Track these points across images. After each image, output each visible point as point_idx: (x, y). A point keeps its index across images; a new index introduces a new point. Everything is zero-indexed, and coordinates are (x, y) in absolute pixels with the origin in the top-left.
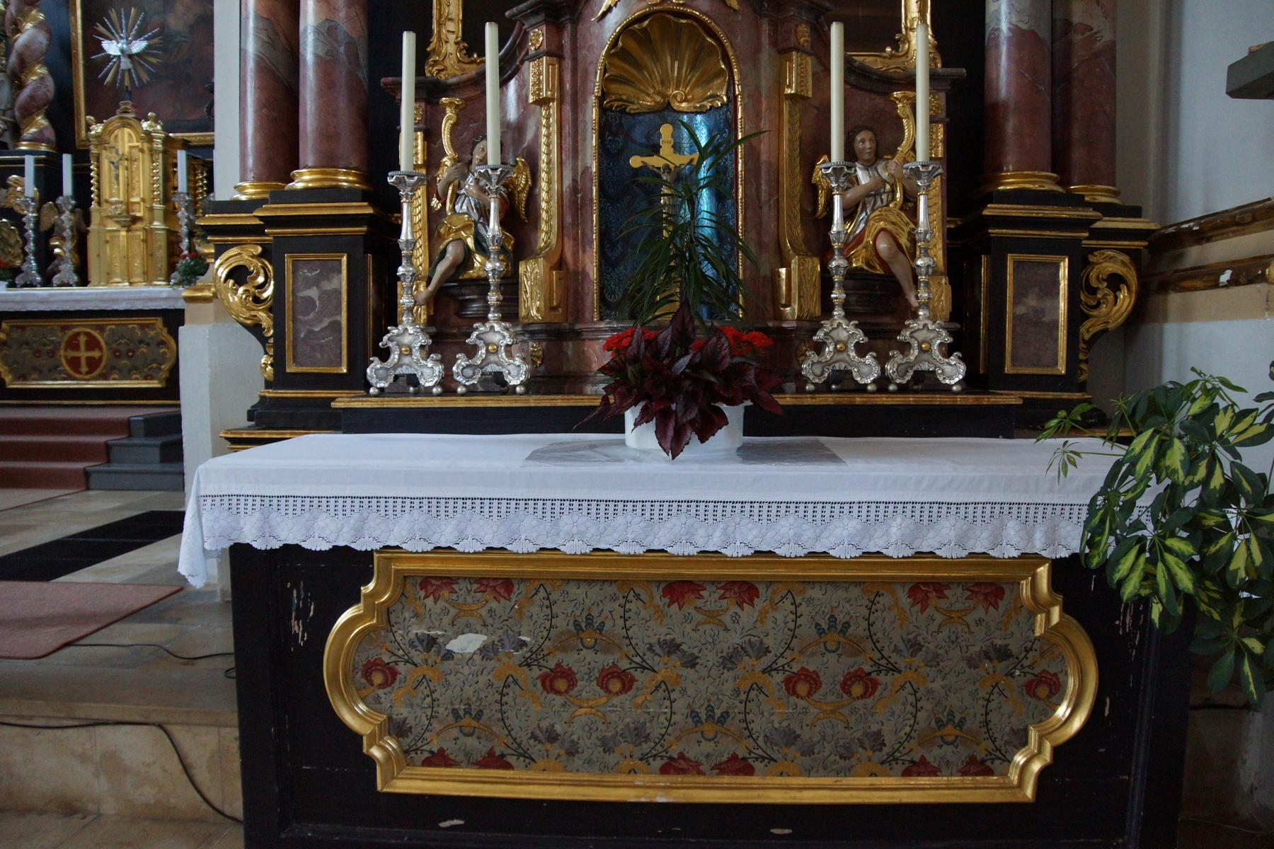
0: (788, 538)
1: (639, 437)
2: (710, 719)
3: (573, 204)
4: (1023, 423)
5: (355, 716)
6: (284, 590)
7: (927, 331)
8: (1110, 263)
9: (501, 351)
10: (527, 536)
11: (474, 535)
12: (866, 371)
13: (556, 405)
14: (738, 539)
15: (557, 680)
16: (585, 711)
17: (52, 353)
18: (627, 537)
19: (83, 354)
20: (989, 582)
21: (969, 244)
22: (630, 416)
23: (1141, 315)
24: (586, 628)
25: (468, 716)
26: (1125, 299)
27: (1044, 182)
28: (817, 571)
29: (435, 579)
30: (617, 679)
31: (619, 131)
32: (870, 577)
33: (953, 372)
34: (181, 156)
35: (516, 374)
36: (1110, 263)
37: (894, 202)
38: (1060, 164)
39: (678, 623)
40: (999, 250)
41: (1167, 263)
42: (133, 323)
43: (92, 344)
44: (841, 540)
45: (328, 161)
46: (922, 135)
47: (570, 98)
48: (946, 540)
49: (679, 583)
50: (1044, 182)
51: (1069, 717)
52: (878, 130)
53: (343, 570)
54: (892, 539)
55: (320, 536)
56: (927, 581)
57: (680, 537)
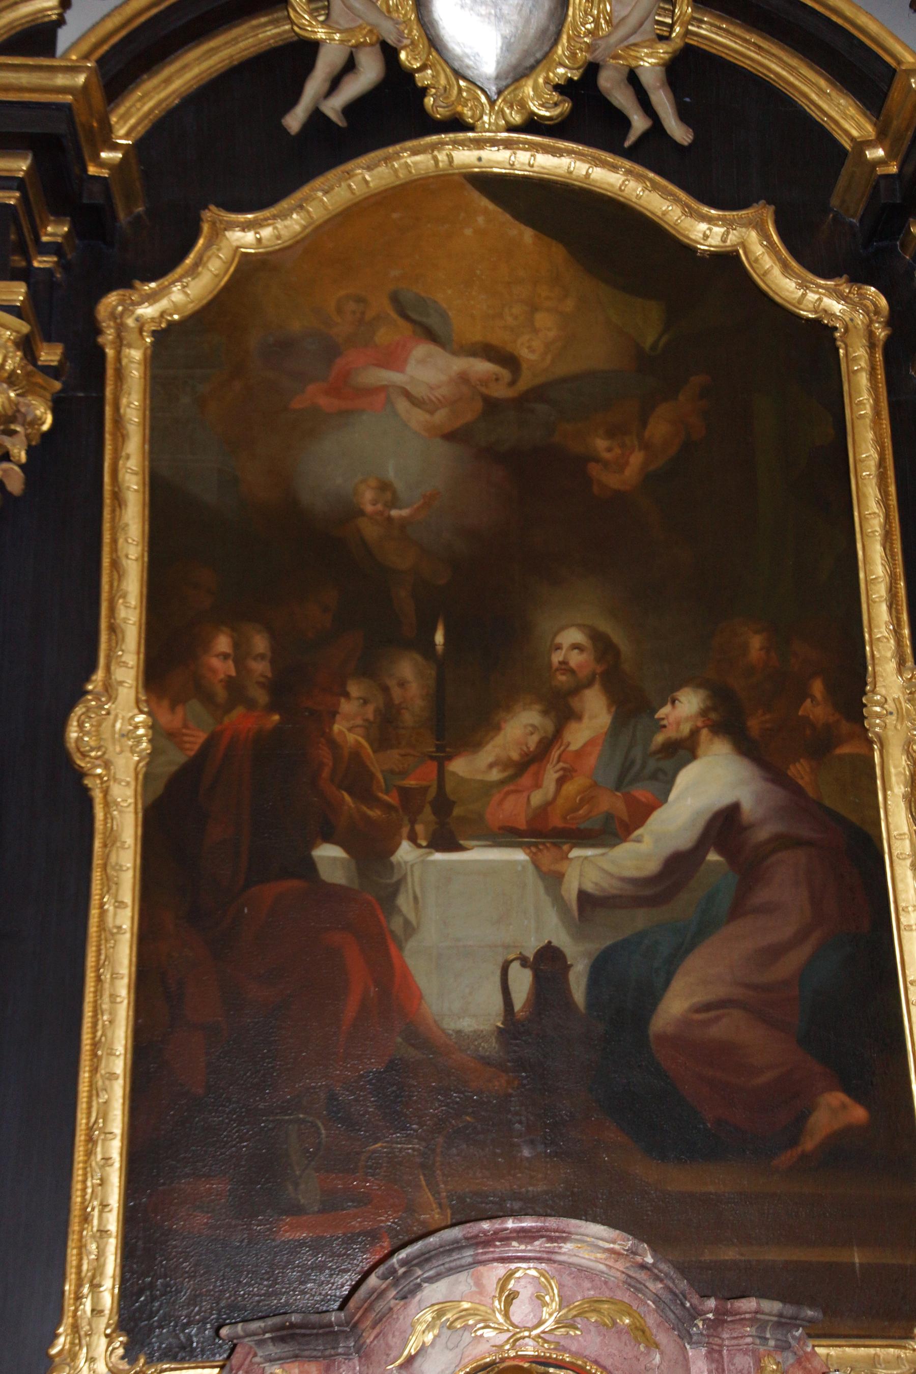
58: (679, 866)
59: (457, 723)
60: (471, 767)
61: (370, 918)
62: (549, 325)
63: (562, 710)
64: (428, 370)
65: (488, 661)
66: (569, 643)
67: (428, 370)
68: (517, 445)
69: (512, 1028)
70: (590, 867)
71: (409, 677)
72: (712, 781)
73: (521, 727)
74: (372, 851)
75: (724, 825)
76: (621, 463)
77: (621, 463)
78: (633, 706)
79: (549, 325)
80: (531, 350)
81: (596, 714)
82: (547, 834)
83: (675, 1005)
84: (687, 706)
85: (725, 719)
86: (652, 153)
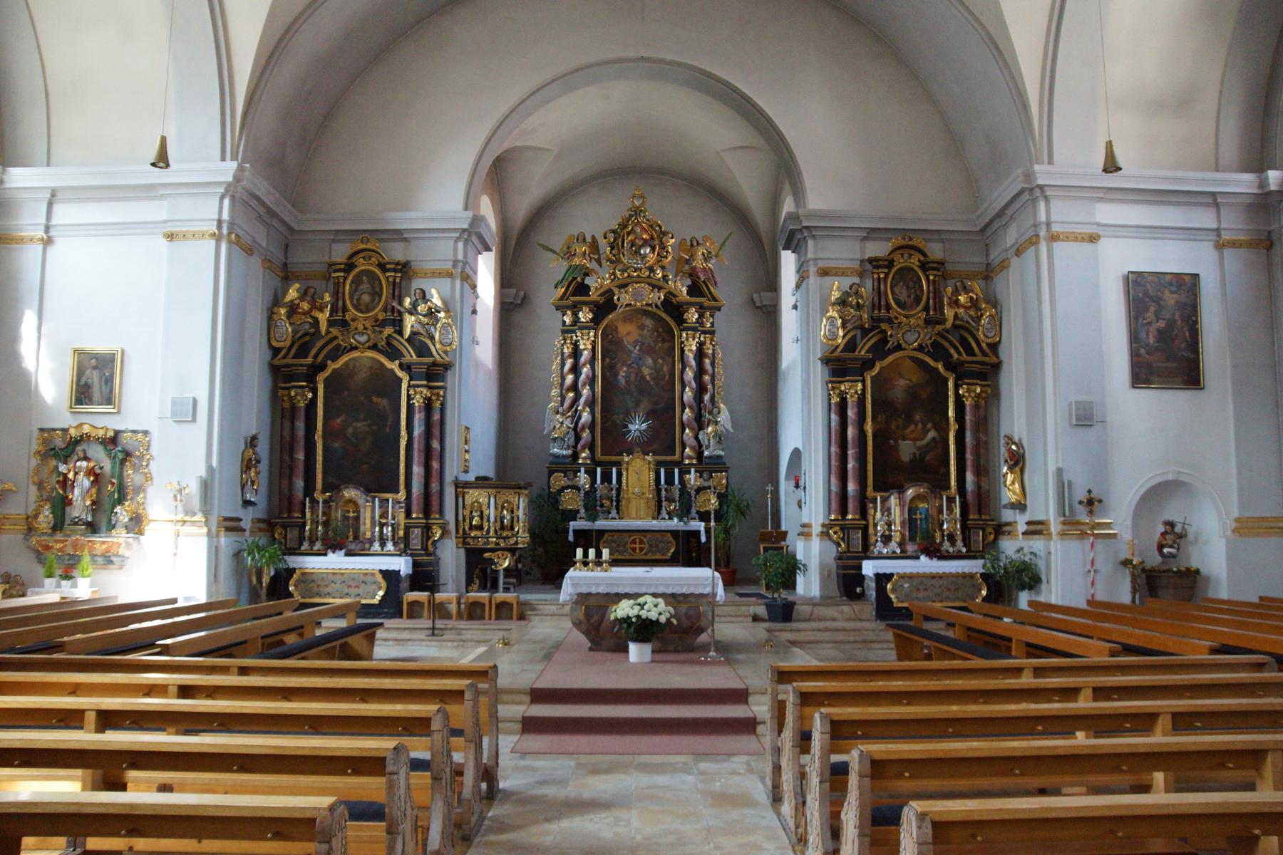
0: (947, 571)
1: (923, 558)
2: (937, 595)
3: (903, 524)
4: (975, 558)
5: (892, 596)
6: (882, 579)
7: (959, 543)
8: (990, 530)
9: (894, 546)
10: (915, 571)
11: (908, 571)
12: (951, 550)
13: (904, 556)
14: (941, 571)
15: (918, 590)
16: (922, 594)
17: (625, 546)
18: (928, 570)
19: (638, 546)
20: (971, 576)
21: (964, 528)
22: (923, 558)
23: (996, 540)
24: (921, 583)
25: (906, 596)
26: (992, 536)
27: (977, 517)
28: (950, 575)
29: (903, 577)
30: (925, 590)
31: (912, 511)
32: (957, 575)
33: (964, 550)
34: (662, 471)
35: (898, 551)
36: (990, 530)
37: (951, 522)
38: (980, 513)
39: (933, 582)
40: (969, 529)
41: (1000, 529)
42: (658, 535)
43: (641, 542)
44: (953, 571)
45: (854, 514)
46: (957, 510)
47: (902, 505)
48: (966, 571)
49: (933, 577)
50: (977, 517)
51: (984, 593)
52: (950, 510)
53: (889, 577)
54: (960, 571)
55: (888, 571)
56: (965, 576)
57: (934, 571)
58: (928, 444)
59: (905, 427)
60: (908, 431)
61: (896, 448)
62: (915, 376)
63: (916, 425)
64: (902, 382)
65: (909, 419)
66: (917, 417)
67: (902, 382)
68: (912, 392)
69: (911, 461)
70: (919, 443)
71: (900, 420)
72: (932, 434)
73: (912, 427)
74: (896, 441)
75: (934, 439)
76: (924, 395)
77: (924, 395)
78: (924, 425)
79: (915, 376)
80: (914, 380)
81: (920, 426)
82: (915, 440)
83: (928, 458)
84: (930, 425)
85: (935, 427)
86: (928, 354)
